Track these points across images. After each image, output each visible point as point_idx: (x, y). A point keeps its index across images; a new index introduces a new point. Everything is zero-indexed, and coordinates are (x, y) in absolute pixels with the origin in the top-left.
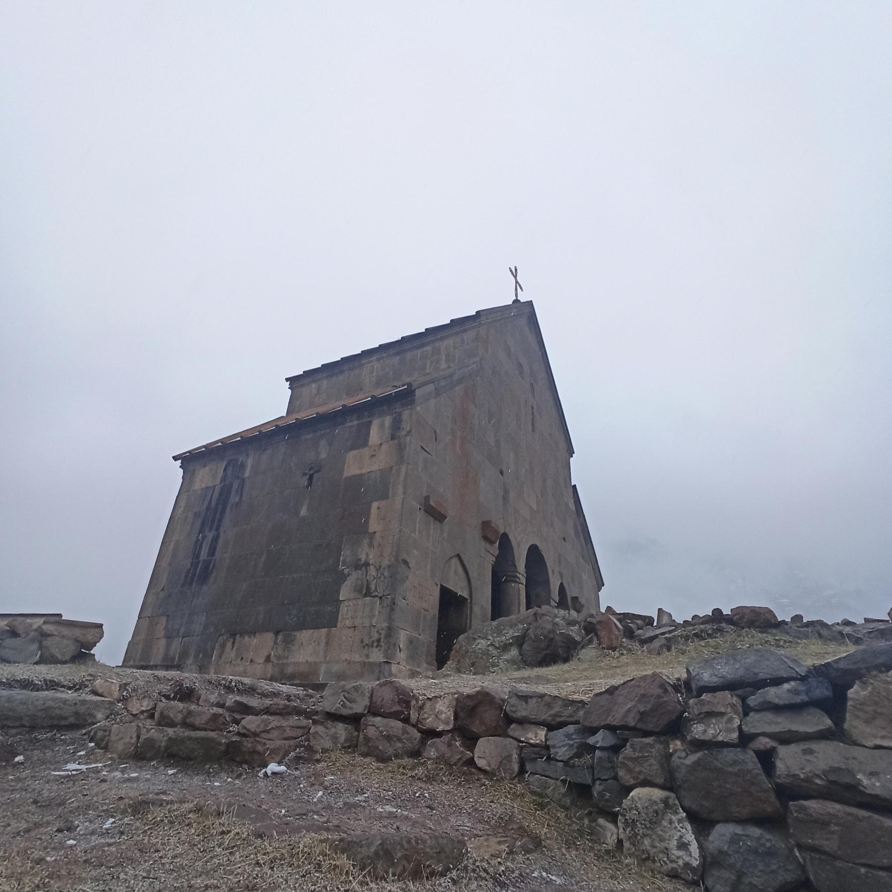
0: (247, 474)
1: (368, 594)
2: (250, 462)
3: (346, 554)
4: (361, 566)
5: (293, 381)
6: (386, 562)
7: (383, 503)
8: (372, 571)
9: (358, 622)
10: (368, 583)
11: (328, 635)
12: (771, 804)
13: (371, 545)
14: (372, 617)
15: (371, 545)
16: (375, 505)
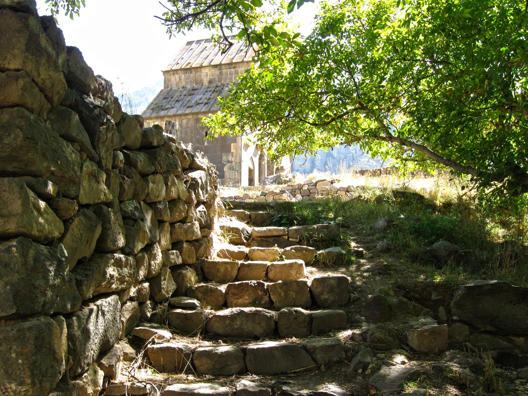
0: (177, 128)
1: (233, 170)
2: (177, 123)
3: (224, 158)
4: (229, 162)
5: (165, 72)
6: (238, 161)
7: (235, 144)
8: (234, 163)
9: (231, 177)
10: (233, 167)
11: (222, 181)
12: (309, 194)
13: (232, 156)
14: (235, 176)
15: (232, 156)
16: (232, 144)
